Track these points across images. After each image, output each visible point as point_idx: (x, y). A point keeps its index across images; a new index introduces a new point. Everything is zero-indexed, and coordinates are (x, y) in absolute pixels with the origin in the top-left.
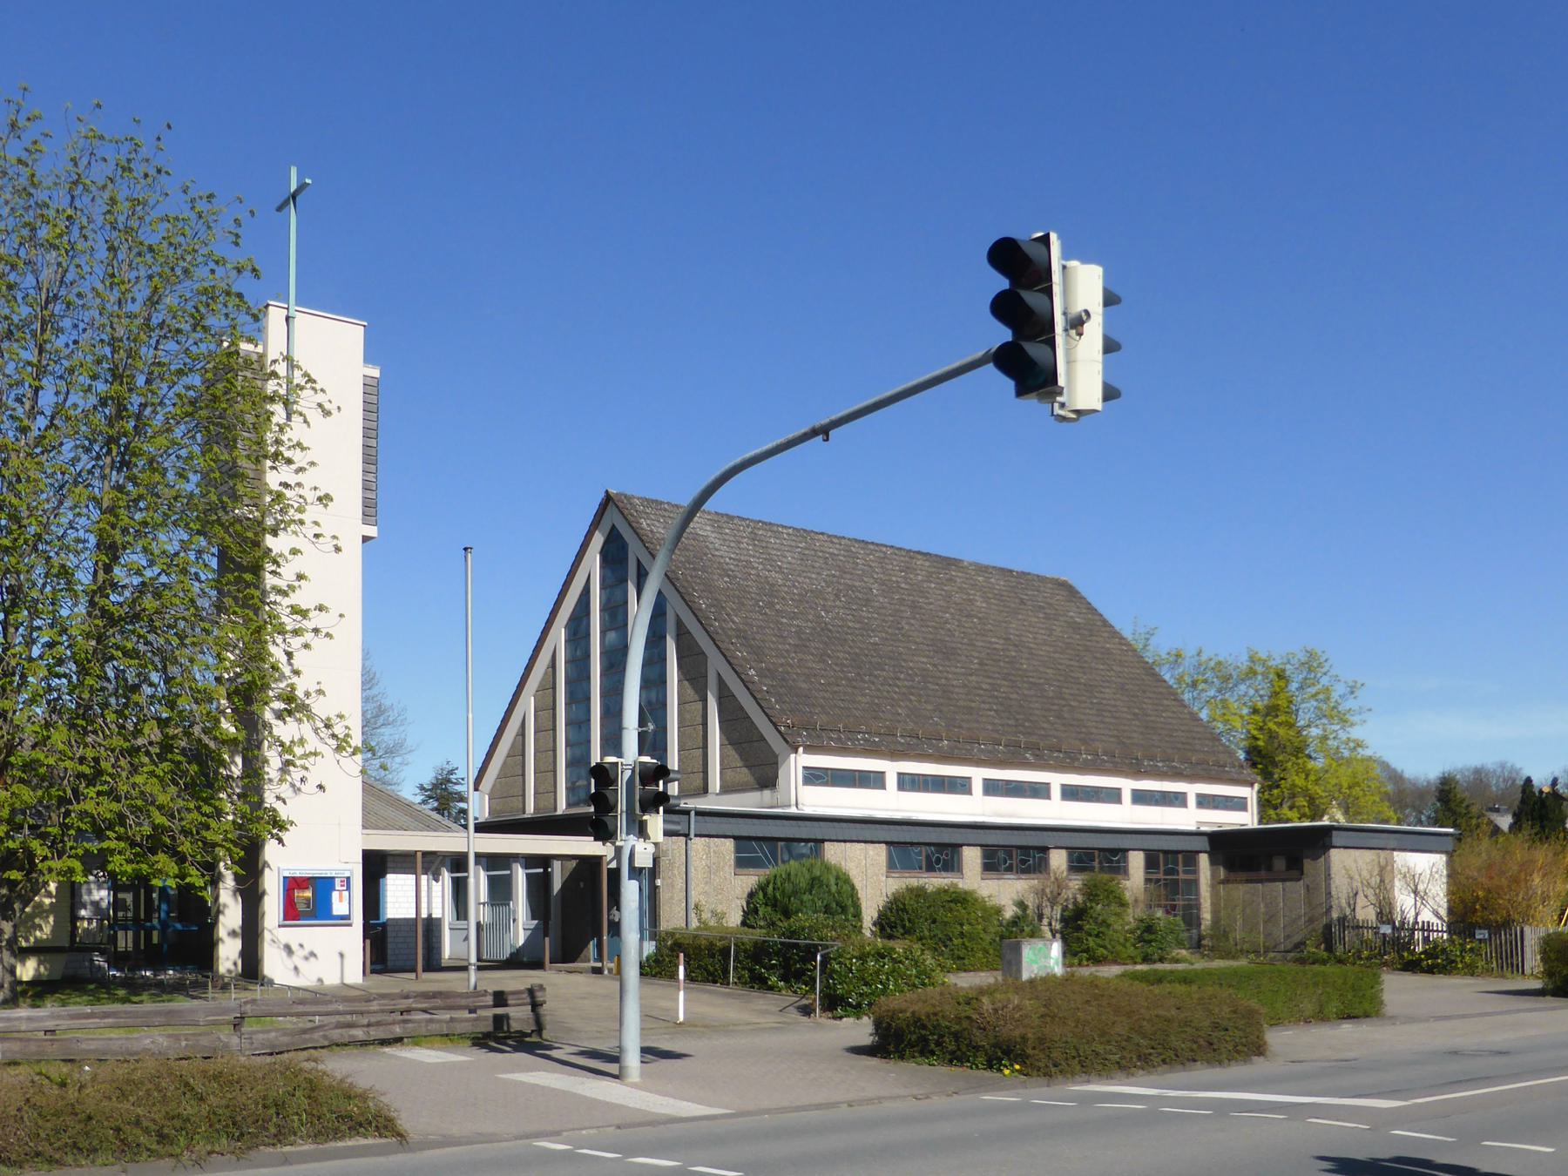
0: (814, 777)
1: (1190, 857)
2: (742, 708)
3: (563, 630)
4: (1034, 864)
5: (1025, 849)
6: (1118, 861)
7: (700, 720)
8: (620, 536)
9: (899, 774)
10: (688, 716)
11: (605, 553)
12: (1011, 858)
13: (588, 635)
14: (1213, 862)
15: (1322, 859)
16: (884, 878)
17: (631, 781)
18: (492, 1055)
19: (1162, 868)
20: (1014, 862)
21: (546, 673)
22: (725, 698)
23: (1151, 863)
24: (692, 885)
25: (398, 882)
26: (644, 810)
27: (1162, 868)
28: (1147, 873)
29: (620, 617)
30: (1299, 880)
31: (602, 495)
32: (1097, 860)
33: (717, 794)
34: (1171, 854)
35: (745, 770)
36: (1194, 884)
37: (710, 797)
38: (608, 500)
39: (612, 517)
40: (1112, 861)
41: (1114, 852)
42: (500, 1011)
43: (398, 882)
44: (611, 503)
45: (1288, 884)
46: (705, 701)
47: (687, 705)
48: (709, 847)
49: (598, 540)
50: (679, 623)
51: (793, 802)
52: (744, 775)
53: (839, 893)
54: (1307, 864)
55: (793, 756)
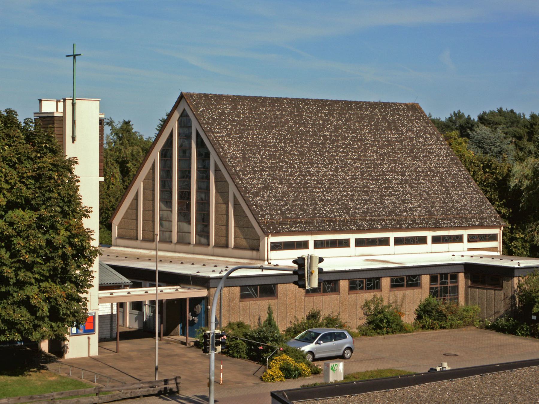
0: (276, 247)
1: (454, 277)
2: (244, 212)
3: (159, 153)
4: (374, 285)
5: (370, 280)
6: (417, 280)
7: (224, 212)
8: (187, 116)
9: (315, 241)
10: (219, 209)
11: (180, 121)
12: (363, 284)
13: (171, 157)
14: (466, 278)
15: (510, 282)
16: (303, 298)
17: (213, 337)
18: (165, 401)
19: (439, 282)
20: (364, 285)
21: (149, 172)
22: (236, 205)
23: (433, 279)
24: (223, 308)
25: (107, 311)
26: (216, 345)
27: (439, 282)
28: (431, 285)
29: (187, 155)
30: (501, 290)
31: (179, 94)
32: (405, 281)
33: (232, 249)
34: (444, 276)
35: (244, 240)
36: (455, 289)
37: (229, 250)
38: (182, 97)
39: (183, 105)
40: (413, 281)
41: (414, 276)
42: (165, 386)
43: (107, 311)
44: (183, 99)
45: (496, 291)
46: (227, 204)
47: (219, 205)
48: (230, 291)
49: (176, 115)
50: (216, 165)
51: (266, 258)
52: (244, 242)
53: (261, 385)
54: (505, 283)
55: (266, 238)
